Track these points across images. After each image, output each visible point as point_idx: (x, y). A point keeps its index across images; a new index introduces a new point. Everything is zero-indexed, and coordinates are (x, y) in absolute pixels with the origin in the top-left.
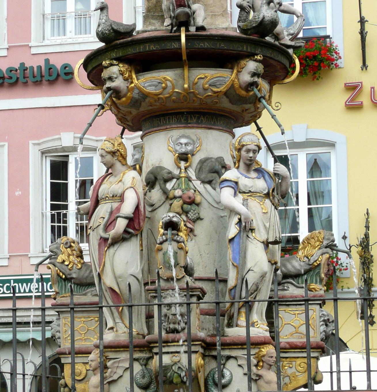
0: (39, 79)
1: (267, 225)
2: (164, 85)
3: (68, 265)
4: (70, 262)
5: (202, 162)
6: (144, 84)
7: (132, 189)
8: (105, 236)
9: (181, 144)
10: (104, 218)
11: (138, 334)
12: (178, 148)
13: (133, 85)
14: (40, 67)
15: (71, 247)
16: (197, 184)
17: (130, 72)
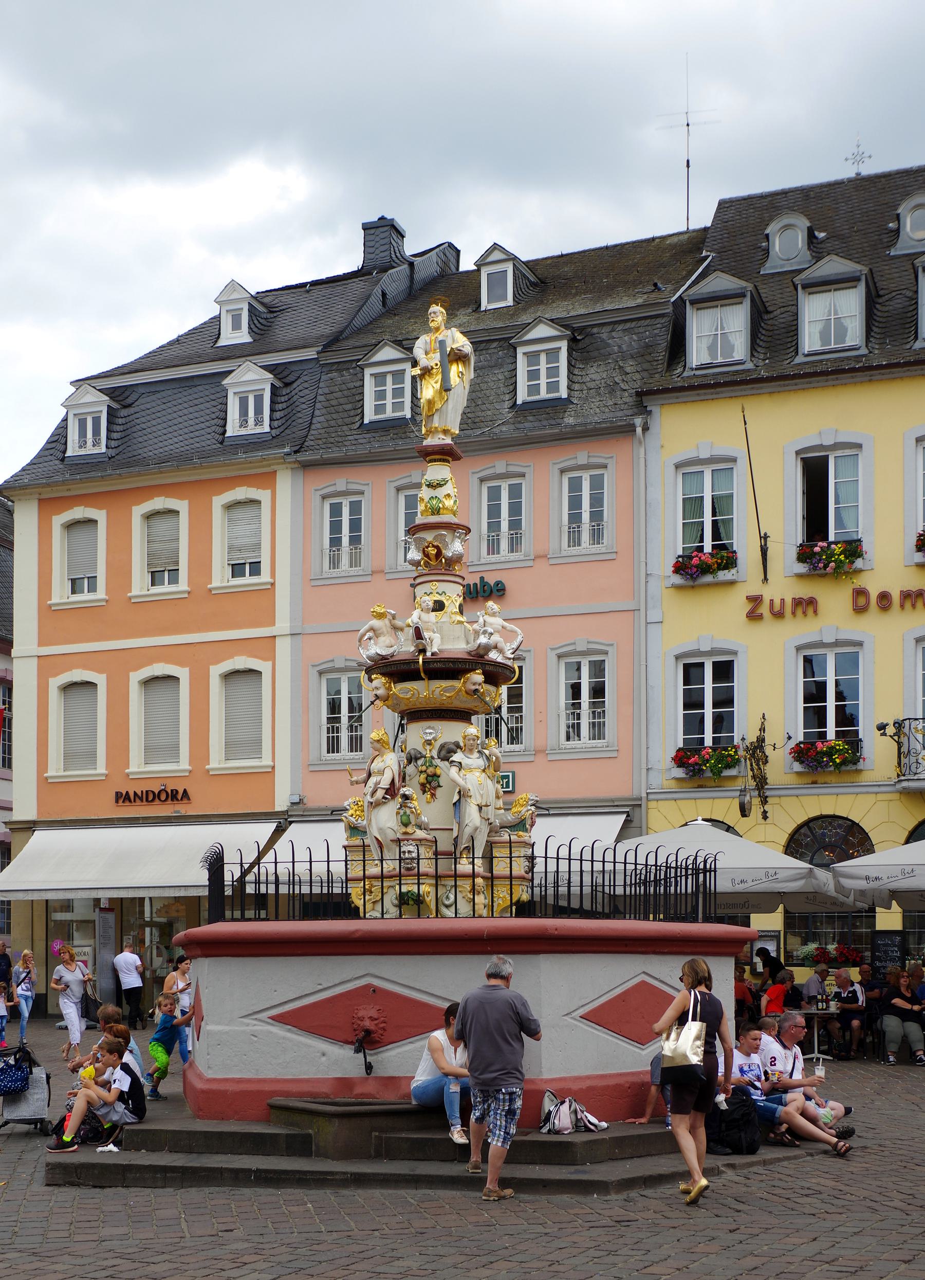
1: (482, 792)
5: (442, 747)
8: (371, 800)
14: (475, 585)
16: (438, 762)
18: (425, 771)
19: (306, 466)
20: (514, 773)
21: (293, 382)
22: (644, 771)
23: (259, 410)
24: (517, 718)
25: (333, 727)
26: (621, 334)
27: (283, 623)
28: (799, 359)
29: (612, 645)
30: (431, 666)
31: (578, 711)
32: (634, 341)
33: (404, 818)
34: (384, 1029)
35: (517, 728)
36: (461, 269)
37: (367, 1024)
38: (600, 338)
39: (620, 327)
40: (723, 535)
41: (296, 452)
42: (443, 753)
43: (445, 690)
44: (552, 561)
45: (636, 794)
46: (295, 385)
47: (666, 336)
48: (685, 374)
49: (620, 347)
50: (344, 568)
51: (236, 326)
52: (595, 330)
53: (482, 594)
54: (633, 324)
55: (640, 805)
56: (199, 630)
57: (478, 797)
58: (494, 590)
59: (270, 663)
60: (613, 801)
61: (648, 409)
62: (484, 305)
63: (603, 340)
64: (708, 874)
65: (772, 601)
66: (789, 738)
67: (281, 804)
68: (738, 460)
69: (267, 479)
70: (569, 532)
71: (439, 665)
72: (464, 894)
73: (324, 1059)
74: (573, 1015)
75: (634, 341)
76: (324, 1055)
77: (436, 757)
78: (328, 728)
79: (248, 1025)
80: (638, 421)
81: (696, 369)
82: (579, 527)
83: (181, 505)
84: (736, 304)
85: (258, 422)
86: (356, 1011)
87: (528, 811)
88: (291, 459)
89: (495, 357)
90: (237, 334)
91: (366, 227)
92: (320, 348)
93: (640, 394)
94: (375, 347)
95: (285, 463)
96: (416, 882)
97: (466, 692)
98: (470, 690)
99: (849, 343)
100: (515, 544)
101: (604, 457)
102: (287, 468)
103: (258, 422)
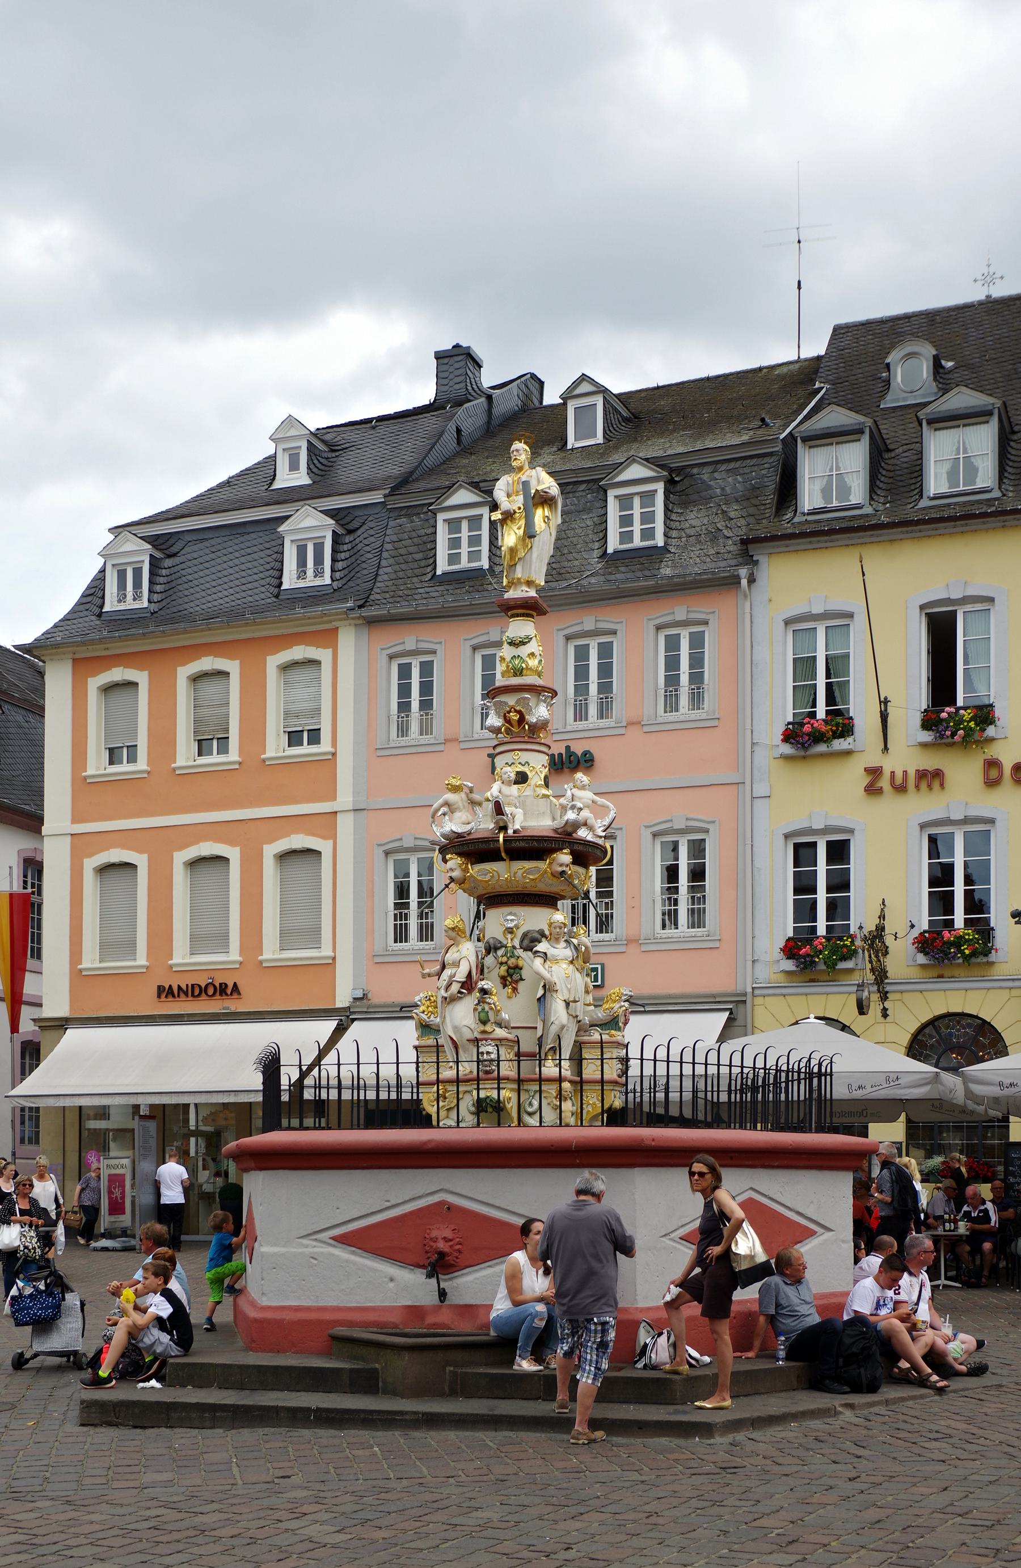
0: (560, 766)
1: (569, 986)
5: (525, 935)
14: (560, 755)
15: (430, 999)
16: (520, 952)
18: (506, 963)
19: (372, 622)
20: (603, 965)
21: (358, 529)
22: (749, 964)
23: (319, 560)
24: (607, 904)
25: (401, 913)
26: (724, 475)
27: (345, 798)
28: (924, 503)
29: (714, 822)
30: (513, 845)
31: (675, 896)
32: (739, 482)
33: (483, 1015)
34: (459, 1251)
35: (607, 915)
36: (545, 403)
37: (441, 1245)
38: (701, 479)
39: (724, 467)
40: (838, 699)
41: (360, 607)
42: (526, 942)
43: (529, 871)
44: (646, 729)
45: (740, 989)
46: (359, 532)
47: (774, 477)
48: (796, 520)
49: (723, 489)
50: (413, 736)
51: (294, 466)
52: (695, 471)
53: (568, 765)
54: (738, 464)
55: (745, 1002)
56: (251, 804)
57: (565, 991)
58: (582, 762)
59: (331, 842)
60: (714, 996)
61: (755, 558)
62: (571, 442)
63: (703, 482)
64: (823, 1078)
65: (893, 773)
66: (912, 926)
67: (342, 1000)
68: (855, 616)
69: (328, 637)
70: (666, 696)
71: (522, 844)
72: (549, 1100)
73: (391, 1285)
74: (672, 1235)
75: (739, 482)
76: (392, 1280)
77: (518, 946)
78: (395, 915)
79: (307, 1246)
80: (743, 572)
81: (808, 514)
82: (676, 690)
83: (232, 666)
84: (853, 441)
85: (318, 573)
86: (428, 1231)
87: (621, 1007)
88: (355, 614)
89: (583, 501)
90: (295, 475)
91: (439, 356)
92: (387, 491)
93: (745, 542)
94: (449, 489)
95: (347, 619)
96: (496, 1086)
97: (552, 874)
98: (557, 872)
99: (980, 483)
100: (604, 710)
101: (704, 613)
102: (350, 625)
103: (318, 573)
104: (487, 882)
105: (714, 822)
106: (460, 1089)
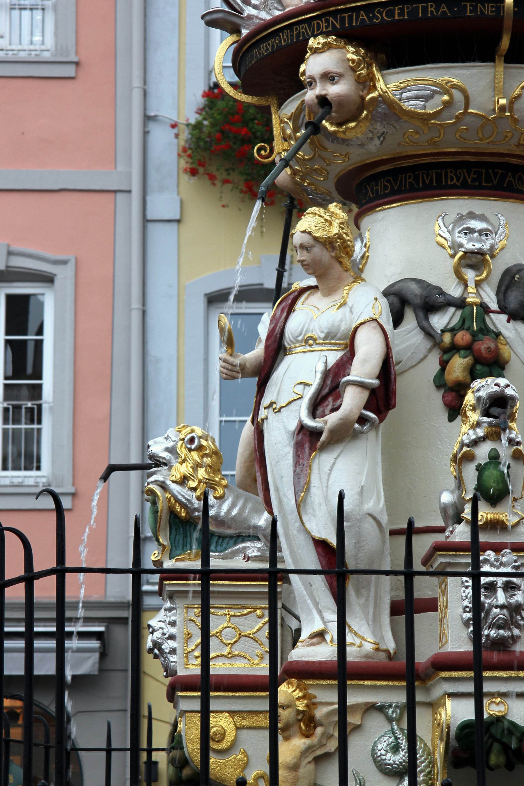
2: (446, 98)
3: (195, 489)
4: (200, 481)
6: (402, 93)
7: (374, 324)
9: (470, 231)
10: (306, 385)
11: (377, 650)
12: (463, 240)
13: (374, 94)
15: (200, 448)
17: (369, 66)
18: (468, 348)
29: (64, 262)
77: (494, 306)
96: (470, 688)
104: (425, 118)
105: (64, 262)
106: (352, 699)
